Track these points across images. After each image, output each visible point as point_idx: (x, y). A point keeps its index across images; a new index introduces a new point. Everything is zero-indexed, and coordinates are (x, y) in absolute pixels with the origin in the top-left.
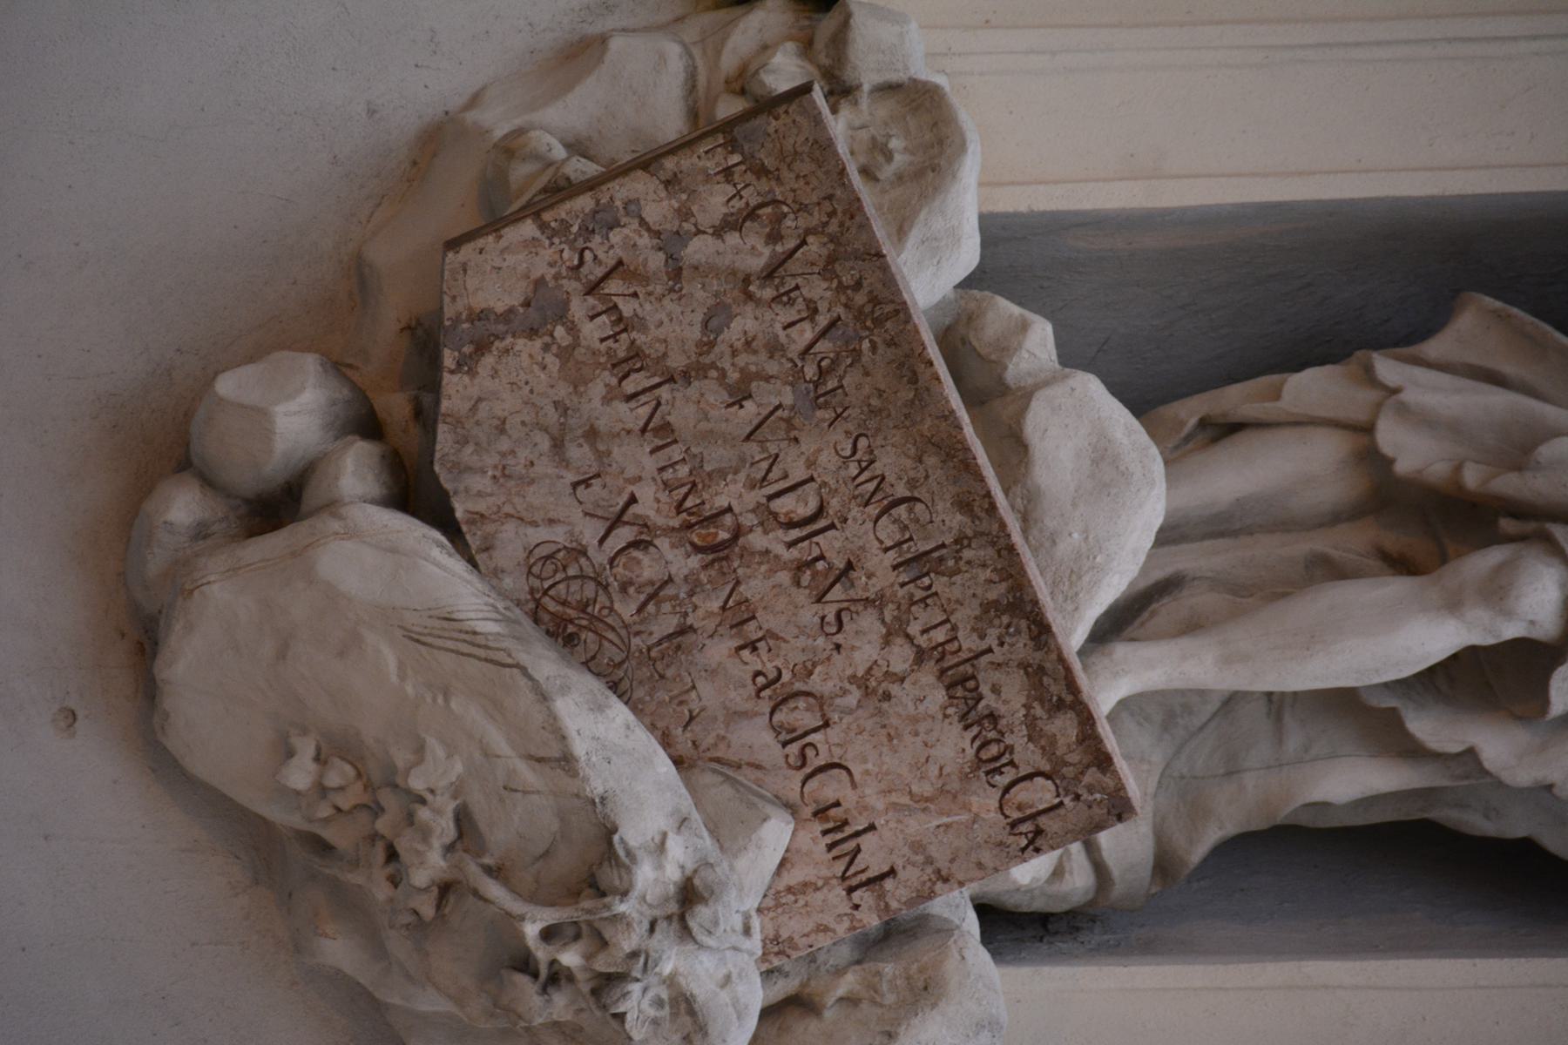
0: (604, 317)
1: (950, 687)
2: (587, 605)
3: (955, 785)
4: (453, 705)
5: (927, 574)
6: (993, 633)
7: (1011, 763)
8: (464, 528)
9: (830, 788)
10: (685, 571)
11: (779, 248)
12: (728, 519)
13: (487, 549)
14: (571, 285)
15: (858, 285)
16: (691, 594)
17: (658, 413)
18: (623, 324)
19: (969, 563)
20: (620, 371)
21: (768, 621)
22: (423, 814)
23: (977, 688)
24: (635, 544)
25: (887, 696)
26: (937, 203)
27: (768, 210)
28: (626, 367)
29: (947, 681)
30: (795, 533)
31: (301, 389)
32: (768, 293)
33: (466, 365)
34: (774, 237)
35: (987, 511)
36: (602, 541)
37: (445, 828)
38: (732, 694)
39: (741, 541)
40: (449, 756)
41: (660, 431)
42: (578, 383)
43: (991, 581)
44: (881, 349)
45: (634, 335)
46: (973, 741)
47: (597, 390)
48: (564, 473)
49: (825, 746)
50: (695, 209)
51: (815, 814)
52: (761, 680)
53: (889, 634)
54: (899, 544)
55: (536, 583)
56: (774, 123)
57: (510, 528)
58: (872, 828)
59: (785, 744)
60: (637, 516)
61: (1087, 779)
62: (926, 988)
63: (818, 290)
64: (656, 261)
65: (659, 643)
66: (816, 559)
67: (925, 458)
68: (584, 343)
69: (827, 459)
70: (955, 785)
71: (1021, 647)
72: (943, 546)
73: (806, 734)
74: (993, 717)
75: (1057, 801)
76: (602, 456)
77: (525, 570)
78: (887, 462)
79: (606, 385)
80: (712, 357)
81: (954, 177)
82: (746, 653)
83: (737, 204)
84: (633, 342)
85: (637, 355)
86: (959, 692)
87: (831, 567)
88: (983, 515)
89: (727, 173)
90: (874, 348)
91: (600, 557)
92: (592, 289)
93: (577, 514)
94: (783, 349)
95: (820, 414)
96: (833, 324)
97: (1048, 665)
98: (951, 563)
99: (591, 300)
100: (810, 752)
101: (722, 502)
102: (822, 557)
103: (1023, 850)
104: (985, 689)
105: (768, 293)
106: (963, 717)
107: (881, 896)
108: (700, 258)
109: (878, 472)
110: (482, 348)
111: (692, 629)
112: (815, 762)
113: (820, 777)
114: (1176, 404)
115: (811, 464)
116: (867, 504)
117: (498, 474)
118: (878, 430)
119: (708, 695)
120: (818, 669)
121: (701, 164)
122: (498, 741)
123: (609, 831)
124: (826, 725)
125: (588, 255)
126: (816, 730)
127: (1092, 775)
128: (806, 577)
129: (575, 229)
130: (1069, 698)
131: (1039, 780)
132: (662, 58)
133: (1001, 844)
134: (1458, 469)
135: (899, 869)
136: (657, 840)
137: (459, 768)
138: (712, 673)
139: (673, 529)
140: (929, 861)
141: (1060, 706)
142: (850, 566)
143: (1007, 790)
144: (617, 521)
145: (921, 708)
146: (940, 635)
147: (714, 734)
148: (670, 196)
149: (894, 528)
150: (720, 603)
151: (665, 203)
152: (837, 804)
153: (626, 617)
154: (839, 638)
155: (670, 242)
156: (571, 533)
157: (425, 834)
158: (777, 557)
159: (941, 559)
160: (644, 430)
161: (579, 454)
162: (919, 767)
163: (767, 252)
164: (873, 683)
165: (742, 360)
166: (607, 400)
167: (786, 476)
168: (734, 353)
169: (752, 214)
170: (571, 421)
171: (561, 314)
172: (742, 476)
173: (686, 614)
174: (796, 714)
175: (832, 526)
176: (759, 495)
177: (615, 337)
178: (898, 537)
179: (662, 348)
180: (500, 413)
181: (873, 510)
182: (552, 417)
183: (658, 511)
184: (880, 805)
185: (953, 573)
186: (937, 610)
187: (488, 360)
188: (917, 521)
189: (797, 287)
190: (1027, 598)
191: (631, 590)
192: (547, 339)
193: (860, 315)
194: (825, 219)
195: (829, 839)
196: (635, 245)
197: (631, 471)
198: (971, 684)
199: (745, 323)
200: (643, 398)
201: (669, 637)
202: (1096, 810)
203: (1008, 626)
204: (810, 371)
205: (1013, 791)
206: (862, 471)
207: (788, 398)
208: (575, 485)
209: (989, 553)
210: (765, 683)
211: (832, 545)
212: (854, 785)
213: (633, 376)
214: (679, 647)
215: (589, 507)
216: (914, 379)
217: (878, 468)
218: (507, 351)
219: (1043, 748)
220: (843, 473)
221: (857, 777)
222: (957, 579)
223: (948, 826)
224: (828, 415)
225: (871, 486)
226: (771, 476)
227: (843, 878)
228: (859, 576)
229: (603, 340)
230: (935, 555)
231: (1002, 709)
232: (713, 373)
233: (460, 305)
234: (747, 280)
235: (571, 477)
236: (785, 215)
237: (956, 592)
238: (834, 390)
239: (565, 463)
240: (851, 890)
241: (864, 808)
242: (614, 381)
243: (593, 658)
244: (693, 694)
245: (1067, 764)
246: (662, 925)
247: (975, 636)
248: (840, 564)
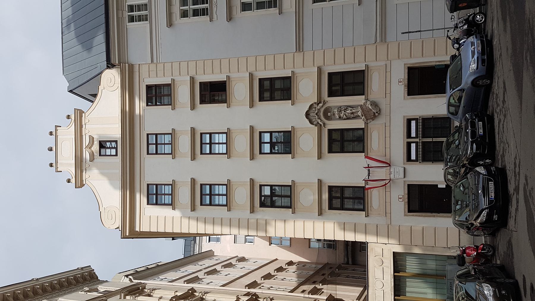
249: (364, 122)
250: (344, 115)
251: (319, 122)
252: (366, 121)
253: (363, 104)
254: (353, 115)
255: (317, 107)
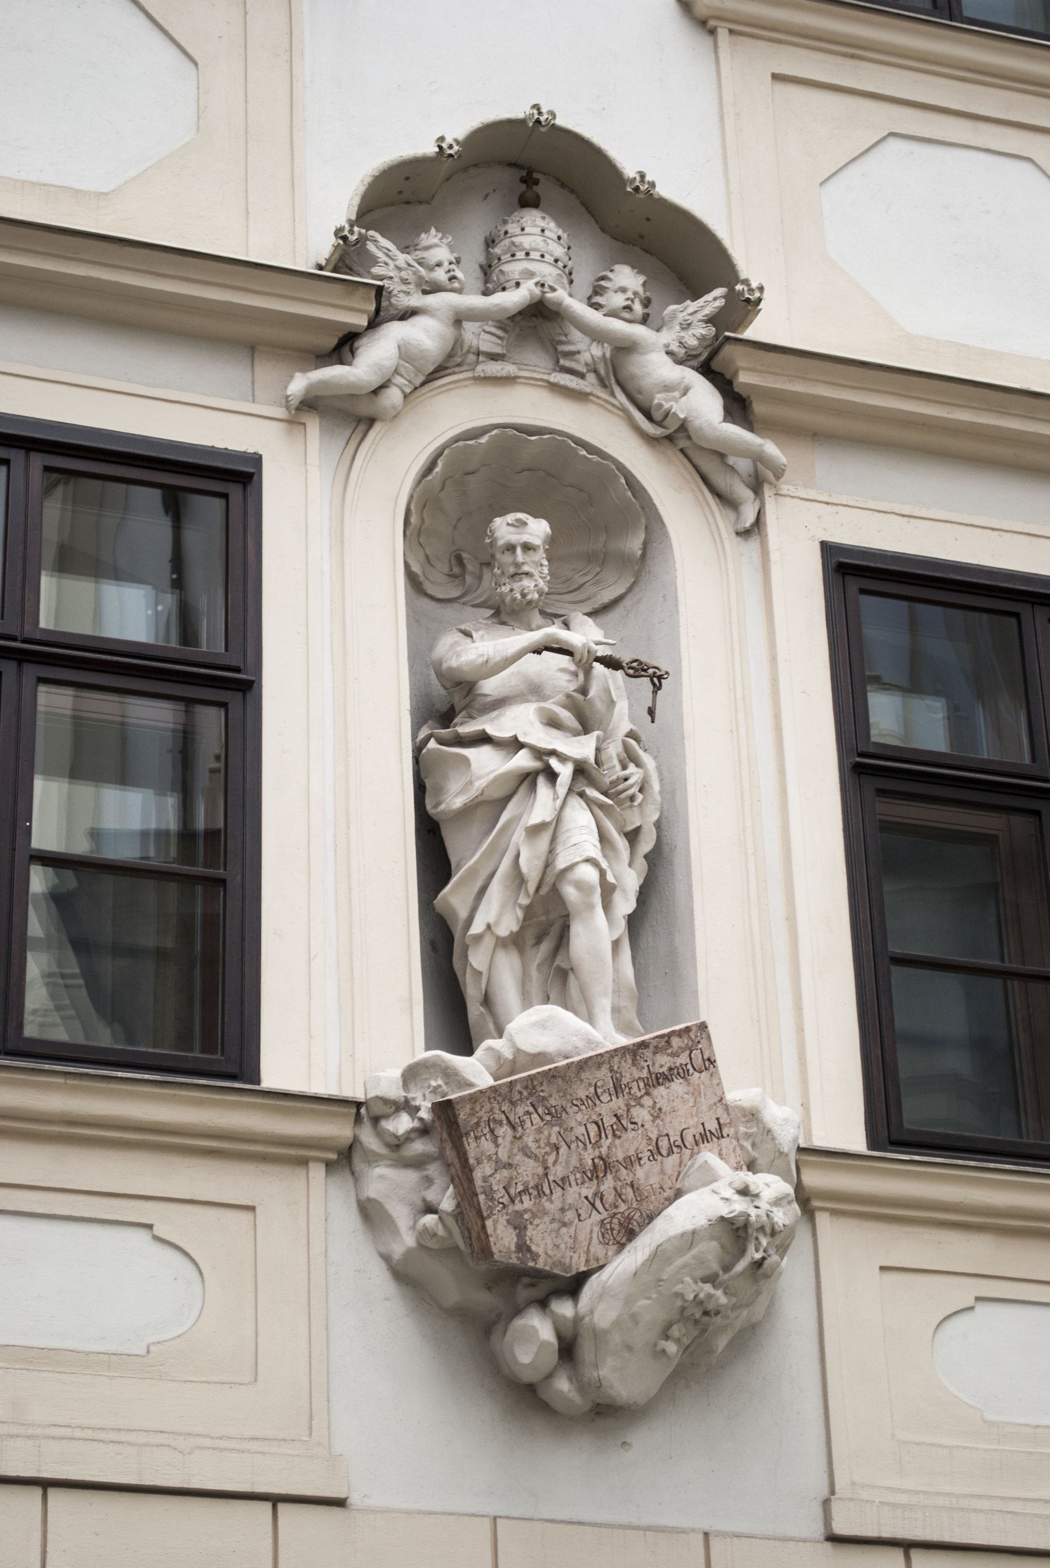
0: (523, 1197)
1: (659, 1084)
2: (620, 1223)
3: (691, 1089)
4: (665, 1278)
5: (621, 1085)
6: (643, 1064)
7: (686, 1065)
8: (590, 1268)
9: (689, 1139)
10: (612, 1181)
11: (505, 1122)
12: (596, 1161)
13: (598, 1260)
14: (511, 1208)
15: (520, 1093)
16: (620, 1180)
17: (558, 1182)
18: (526, 1191)
19: (619, 1068)
20: (542, 1195)
21: (632, 1152)
22: (702, 1296)
23: (660, 1073)
24: (602, 1200)
25: (660, 1109)
26: (460, 1069)
27: (491, 1124)
28: (541, 1192)
29: (656, 1085)
30: (603, 1135)
31: (533, 1328)
32: (520, 1129)
33: (535, 1257)
34: (501, 1123)
35: (602, 1057)
36: (599, 1213)
37: (708, 1288)
38: (655, 1170)
39: (604, 1157)
40: (682, 1282)
41: (563, 1183)
42: (545, 1213)
43: (625, 1061)
44: (543, 1088)
45: (530, 1186)
46: (677, 1079)
47: (547, 1205)
48: (575, 1224)
49: (675, 1137)
50: (488, 1154)
51: (697, 1145)
52: (651, 1158)
53: (639, 1104)
54: (610, 1095)
55: (611, 1242)
56: (461, 1116)
57: (592, 1249)
58: (703, 1124)
59: (673, 1153)
60: (592, 1198)
61: (693, 1037)
62: (753, 1115)
63: (520, 1110)
64: (505, 1173)
65: (635, 1196)
66: (612, 1128)
67: (582, 1078)
68: (531, 1208)
69: (579, 1117)
70: (691, 1089)
71: (648, 1053)
72: (612, 1077)
73: (670, 1144)
74: (670, 1069)
75: (699, 1051)
76: (570, 1207)
77: (606, 1246)
78: (582, 1093)
79: (546, 1201)
80: (540, 1156)
81: (450, 1061)
82: (642, 1162)
83: (488, 1136)
84: (532, 1188)
85: (537, 1187)
86: (661, 1081)
87: (615, 1123)
88: (603, 1059)
89: (477, 1138)
90: (542, 1091)
91: (605, 1214)
92: (512, 1201)
93: (589, 1221)
94: (540, 1128)
95: (563, 1117)
96: (533, 1106)
97: (655, 1044)
98: (618, 1075)
99: (516, 1202)
100: (676, 1144)
101: (590, 1162)
102: (612, 1126)
103: (714, 1067)
104: (661, 1071)
105: (520, 1129)
106: (669, 1081)
107: (725, 1125)
108: (506, 1155)
109: (585, 1097)
110: (529, 1250)
111: (632, 1182)
112: (679, 1143)
113: (685, 1141)
114: (470, 1016)
115: (580, 1124)
116: (595, 1104)
117: (573, 1250)
118: (571, 1095)
119: (654, 1180)
120: (649, 1134)
121: (473, 1148)
122: (680, 1262)
123: (722, 1218)
124: (667, 1135)
125: (501, 1200)
126: (669, 1140)
127: (692, 1034)
128: (617, 1133)
129: (491, 1204)
130: (666, 1038)
131: (692, 1055)
132: (382, 1177)
133: (712, 1075)
134: (520, 906)
135: (717, 1116)
136: (724, 1201)
137: (688, 1279)
138: (647, 1177)
139: (598, 1183)
140: (715, 1104)
141: (668, 1042)
142: (616, 1115)
143: (694, 1069)
144: (593, 1205)
145: (665, 1097)
146: (642, 1085)
147: (668, 1180)
148: (483, 1163)
149: (604, 1094)
150: (624, 1169)
151: (485, 1165)
152: (694, 1136)
153: (626, 1208)
154: (640, 1125)
155: (501, 1166)
156: (595, 1224)
157: (710, 1296)
158: (610, 1144)
159: (616, 1079)
160: (563, 1189)
161: (570, 1215)
162: (684, 1102)
163: (505, 1127)
164: (655, 1114)
165: (543, 1145)
166: (552, 1202)
167: (583, 1135)
168: (539, 1147)
169: (492, 1131)
170: (558, 1217)
171: (519, 1214)
172: (582, 1152)
173: (627, 1184)
174: (664, 1146)
175: (602, 1119)
176: (589, 1146)
177: (530, 1195)
178: (607, 1094)
179: (536, 1176)
180: (552, 1246)
181: (598, 1102)
182: (555, 1225)
183: (591, 1188)
184: (696, 1119)
185: (621, 1075)
186: (633, 1084)
187: (534, 1248)
188: (603, 1086)
189: (519, 1118)
190: (632, 1048)
191: (617, 1204)
192: (528, 1222)
193: (531, 1094)
194: (496, 1102)
195: (706, 1142)
196: (499, 1180)
197: (577, 1196)
198: (659, 1075)
199: (529, 1140)
200: (552, 1187)
201: (634, 1192)
202: (703, 1036)
203: (641, 1057)
204: (548, 1118)
205: (695, 1066)
206: (584, 1104)
207: (556, 1129)
208: (580, 1220)
209: (616, 1059)
210: (652, 1157)
211: (609, 1120)
212: (688, 1128)
213: (544, 1189)
214: (638, 1189)
215: (588, 1216)
216: (554, 1077)
217: (584, 1098)
218: (531, 1239)
219: (682, 1052)
220: (584, 1112)
221: (686, 1126)
222: (623, 1074)
223: (705, 1095)
224: (564, 1115)
225: (590, 1102)
226: (583, 1141)
227: (718, 1138)
228: (620, 1112)
229: (531, 1200)
230: (615, 1081)
231: (668, 1065)
232: (546, 1157)
233: (513, 1256)
234: (515, 1137)
235: (577, 1220)
236: (494, 1118)
237: (628, 1075)
238: (556, 1110)
239: (571, 1223)
240: (723, 1137)
241: (696, 1126)
242: (545, 1198)
243: (638, 1224)
244: (654, 1186)
245: (688, 1044)
246: (756, 1203)
247: (643, 1071)
248: (615, 1119)
249: (395, 1091)
250: (523, 760)
251: (394, 333)
252: (403, 1124)
253: (737, 1094)
254: (508, 926)
255: (669, 337)
